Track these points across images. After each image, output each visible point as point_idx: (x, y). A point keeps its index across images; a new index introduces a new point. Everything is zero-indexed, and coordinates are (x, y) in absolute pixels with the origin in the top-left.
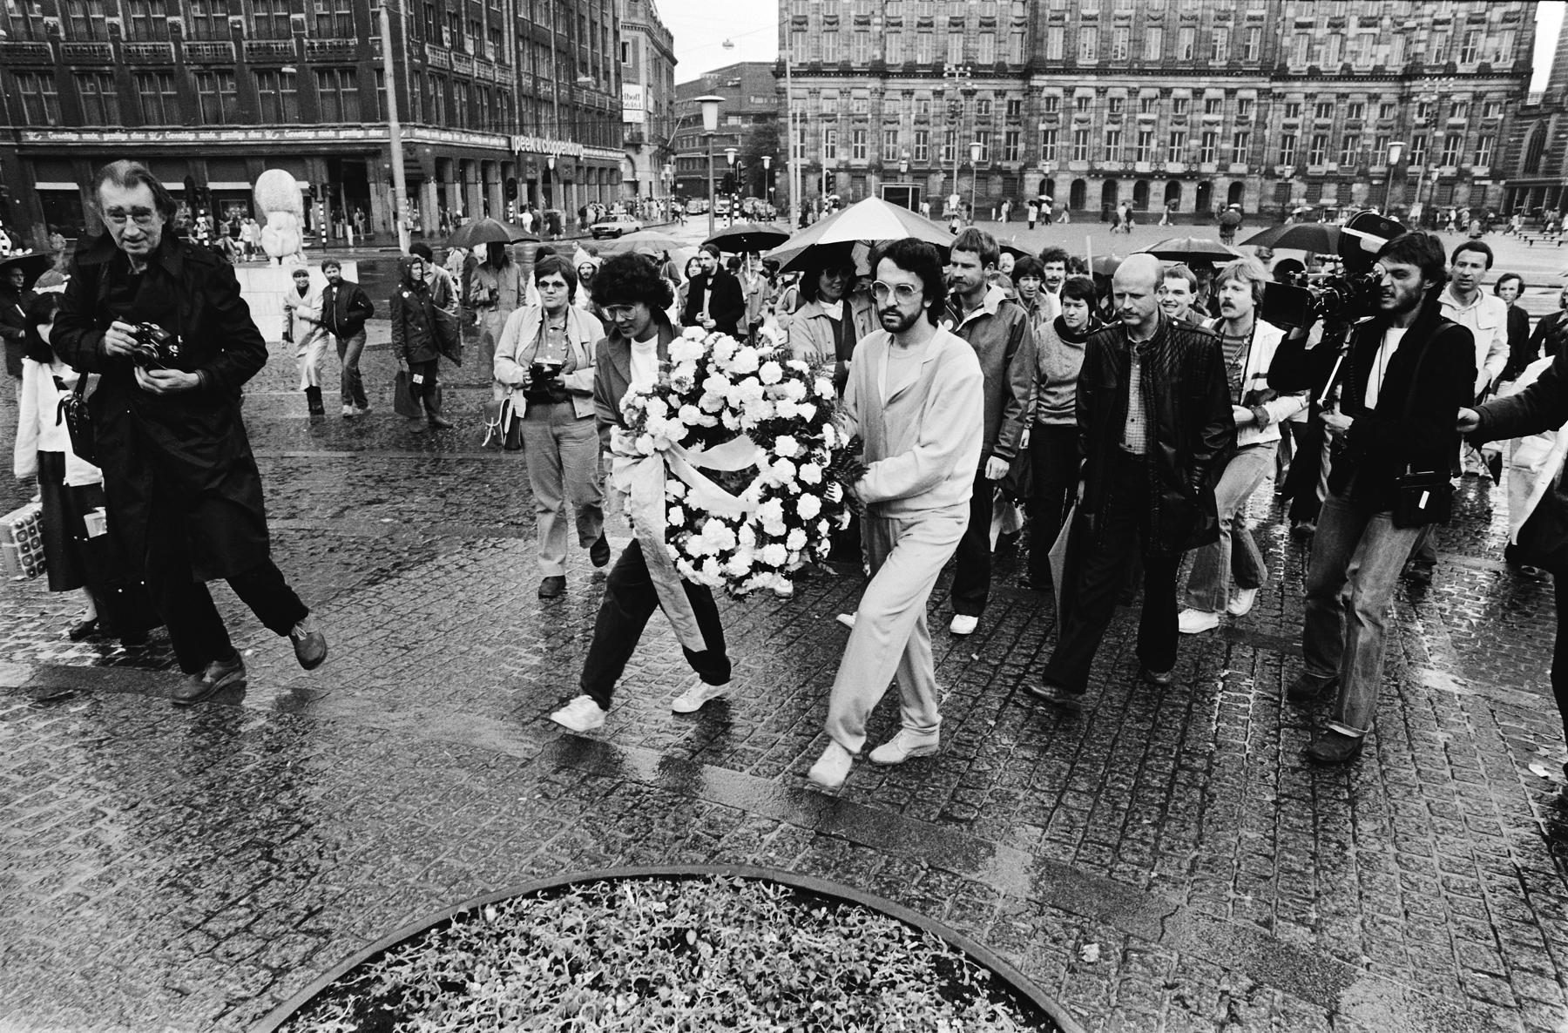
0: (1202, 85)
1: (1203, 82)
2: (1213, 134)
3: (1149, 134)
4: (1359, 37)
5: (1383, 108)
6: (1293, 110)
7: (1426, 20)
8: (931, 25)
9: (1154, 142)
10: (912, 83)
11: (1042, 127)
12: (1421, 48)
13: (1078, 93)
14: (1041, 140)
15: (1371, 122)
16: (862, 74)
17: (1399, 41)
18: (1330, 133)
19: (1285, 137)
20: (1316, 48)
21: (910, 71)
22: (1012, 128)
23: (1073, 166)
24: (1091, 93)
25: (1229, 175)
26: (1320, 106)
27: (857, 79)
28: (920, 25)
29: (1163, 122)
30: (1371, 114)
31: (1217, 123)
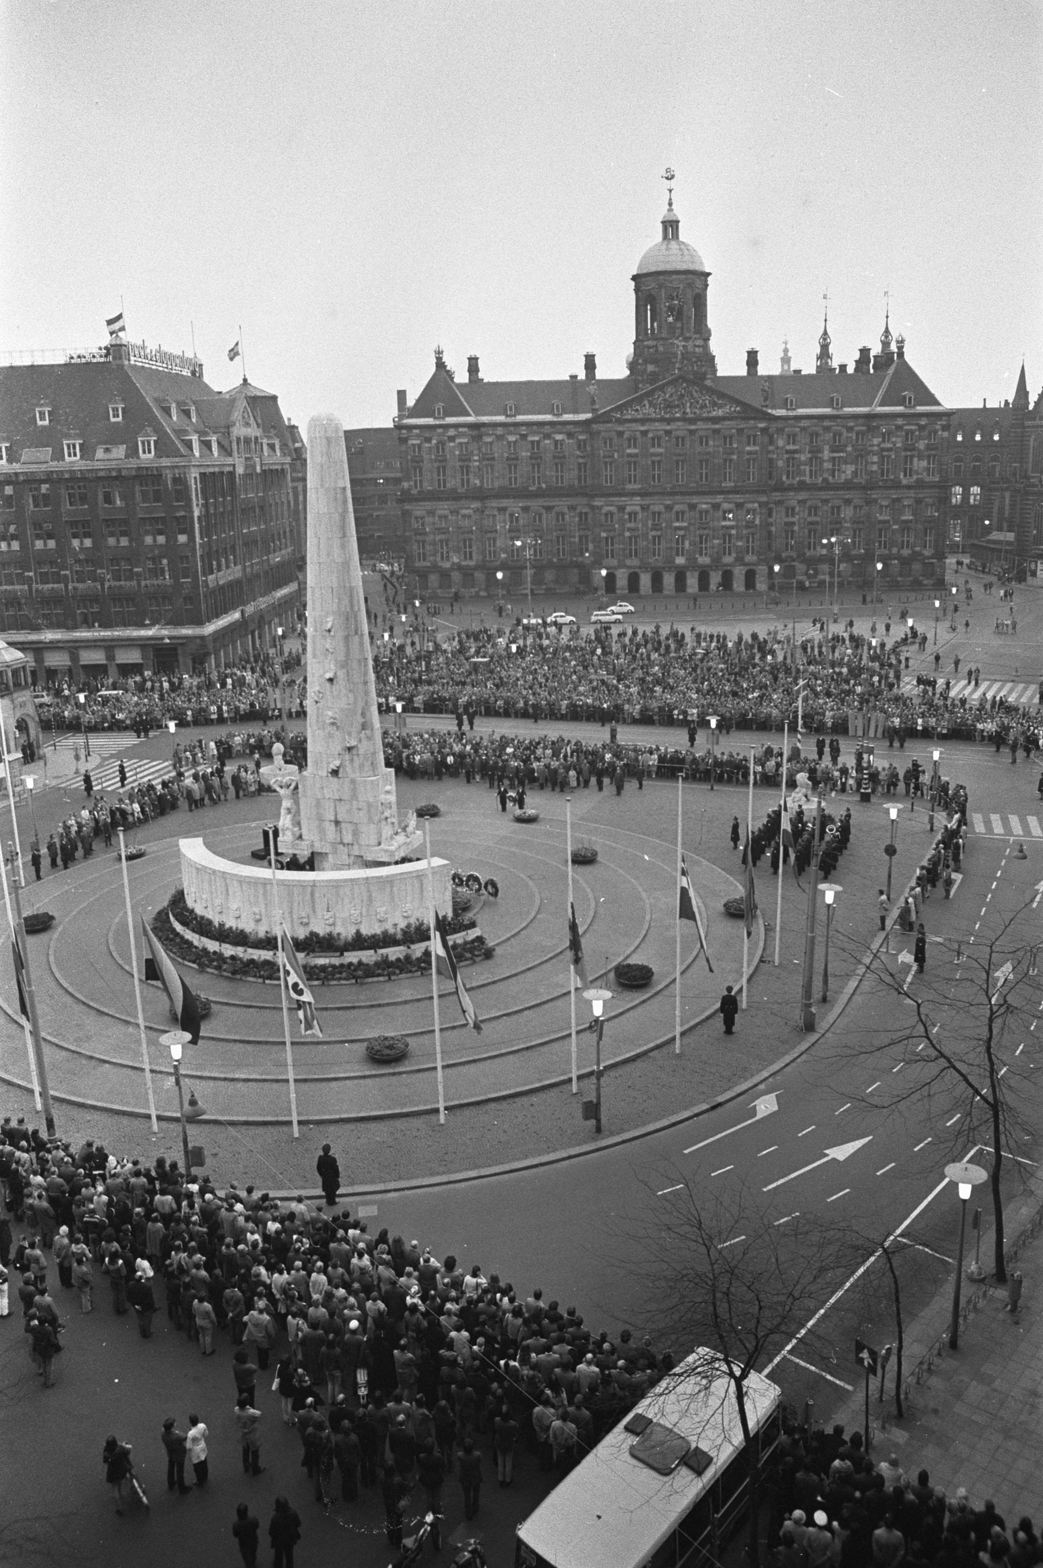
1: (719, 499)
2: (730, 536)
5: (855, 507)
6: (790, 511)
8: (517, 459)
9: (687, 543)
10: (505, 503)
11: (604, 535)
12: (875, 468)
13: (628, 509)
14: (603, 544)
16: (467, 498)
19: (787, 532)
21: (503, 493)
22: (582, 533)
23: (628, 562)
24: (638, 508)
25: (745, 565)
26: (810, 509)
27: (463, 502)
28: (508, 459)
30: (847, 513)
31: (732, 527)
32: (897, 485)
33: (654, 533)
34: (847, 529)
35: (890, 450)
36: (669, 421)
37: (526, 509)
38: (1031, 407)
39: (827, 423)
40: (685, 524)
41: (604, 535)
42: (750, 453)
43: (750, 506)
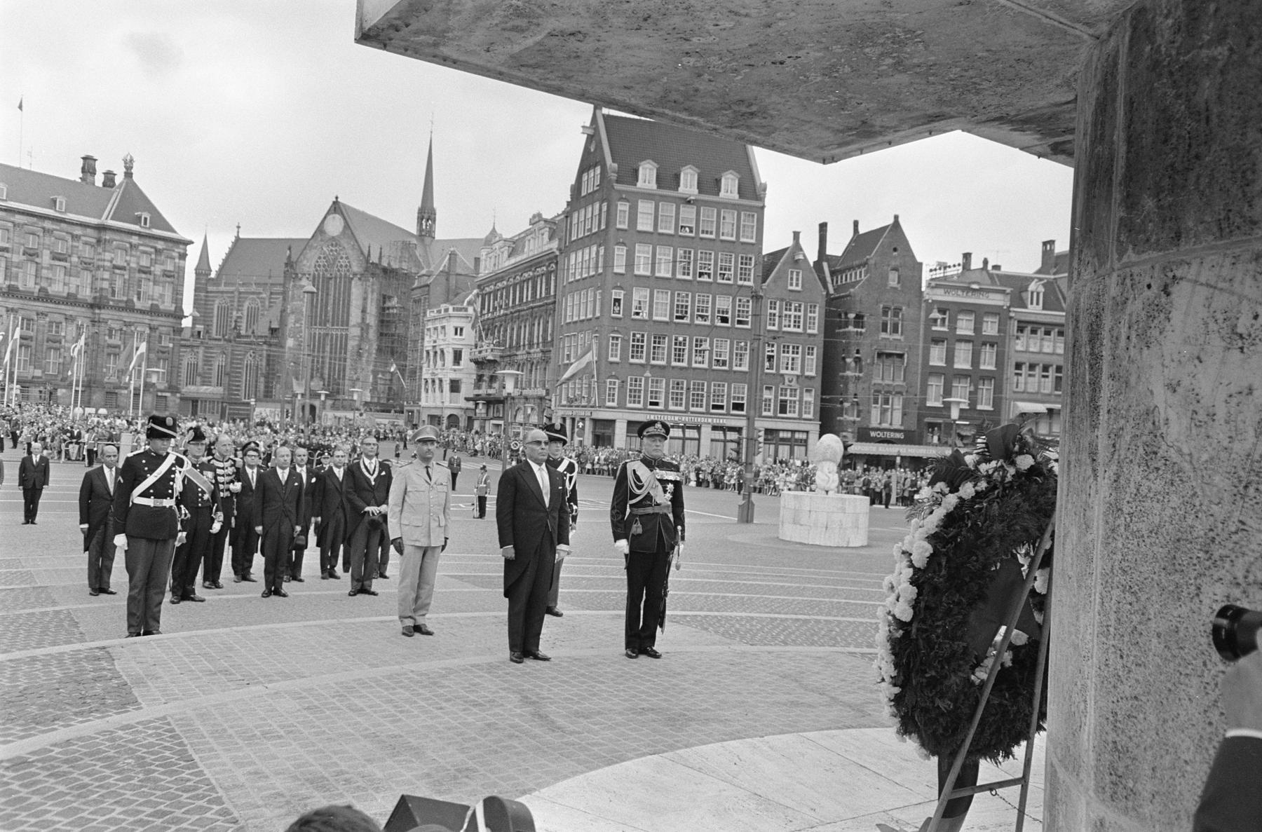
4: (51, 267)
12: (106, 285)
17: (87, 277)
18: (33, 344)
20: (14, 270)
32: (129, 307)
35: (123, 268)
38: (213, 275)
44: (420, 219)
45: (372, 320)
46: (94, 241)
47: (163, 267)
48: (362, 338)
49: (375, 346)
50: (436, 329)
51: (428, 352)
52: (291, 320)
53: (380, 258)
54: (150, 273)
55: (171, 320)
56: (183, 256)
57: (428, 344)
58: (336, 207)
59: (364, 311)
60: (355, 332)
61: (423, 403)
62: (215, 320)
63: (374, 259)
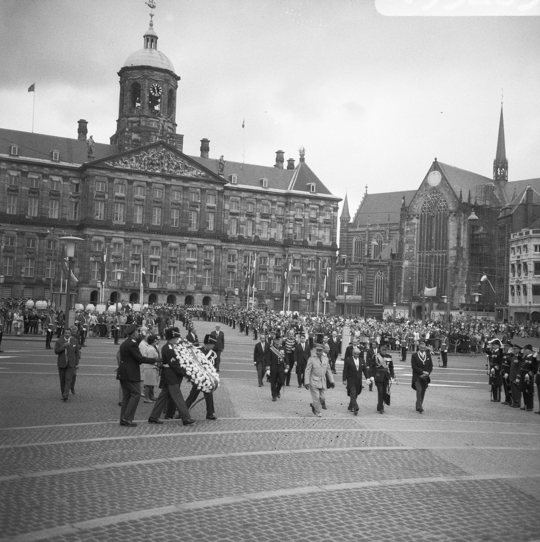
0: (185, 241)
1: (185, 240)
2: (192, 269)
3: (156, 267)
4: (261, 223)
5: (276, 259)
6: (232, 257)
7: (292, 218)
8: (17, 191)
11: (92, 259)
12: (291, 231)
13: (114, 240)
15: (271, 267)
17: (280, 227)
19: (229, 272)
20: (241, 226)
24: (122, 240)
25: (202, 293)
29: (164, 260)
31: (194, 263)
32: (305, 245)
33: (133, 262)
34: (270, 274)
35: (300, 220)
36: (151, 175)
37: (21, 234)
38: (351, 221)
39: (259, 197)
40: (159, 257)
41: (92, 259)
42: (209, 208)
43: (208, 248)
44: (496, 168)
45: (464, 244)
46: (283, 204)
47: (324, 218)
48: (458, 258)
49: (467, 263)
50: (519, 247)
51: (513, 265)
52: (406, 247)
53: (469, 199)
54: (316, 222)
55: (330, 252)
56: (336, 209)
57: (513, 259)
58: (436, 166)
59: (458, 238)
60: (452, 253)
61: (510, 304)
62: (354, 250)
63: (465, 200)
